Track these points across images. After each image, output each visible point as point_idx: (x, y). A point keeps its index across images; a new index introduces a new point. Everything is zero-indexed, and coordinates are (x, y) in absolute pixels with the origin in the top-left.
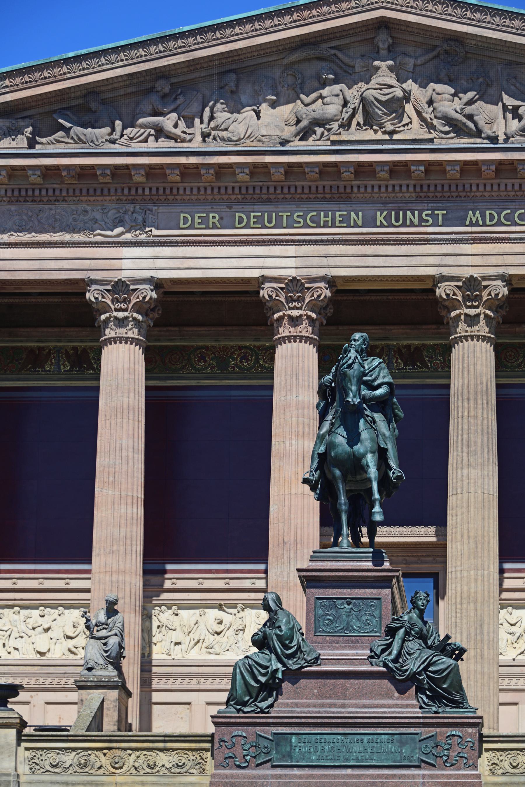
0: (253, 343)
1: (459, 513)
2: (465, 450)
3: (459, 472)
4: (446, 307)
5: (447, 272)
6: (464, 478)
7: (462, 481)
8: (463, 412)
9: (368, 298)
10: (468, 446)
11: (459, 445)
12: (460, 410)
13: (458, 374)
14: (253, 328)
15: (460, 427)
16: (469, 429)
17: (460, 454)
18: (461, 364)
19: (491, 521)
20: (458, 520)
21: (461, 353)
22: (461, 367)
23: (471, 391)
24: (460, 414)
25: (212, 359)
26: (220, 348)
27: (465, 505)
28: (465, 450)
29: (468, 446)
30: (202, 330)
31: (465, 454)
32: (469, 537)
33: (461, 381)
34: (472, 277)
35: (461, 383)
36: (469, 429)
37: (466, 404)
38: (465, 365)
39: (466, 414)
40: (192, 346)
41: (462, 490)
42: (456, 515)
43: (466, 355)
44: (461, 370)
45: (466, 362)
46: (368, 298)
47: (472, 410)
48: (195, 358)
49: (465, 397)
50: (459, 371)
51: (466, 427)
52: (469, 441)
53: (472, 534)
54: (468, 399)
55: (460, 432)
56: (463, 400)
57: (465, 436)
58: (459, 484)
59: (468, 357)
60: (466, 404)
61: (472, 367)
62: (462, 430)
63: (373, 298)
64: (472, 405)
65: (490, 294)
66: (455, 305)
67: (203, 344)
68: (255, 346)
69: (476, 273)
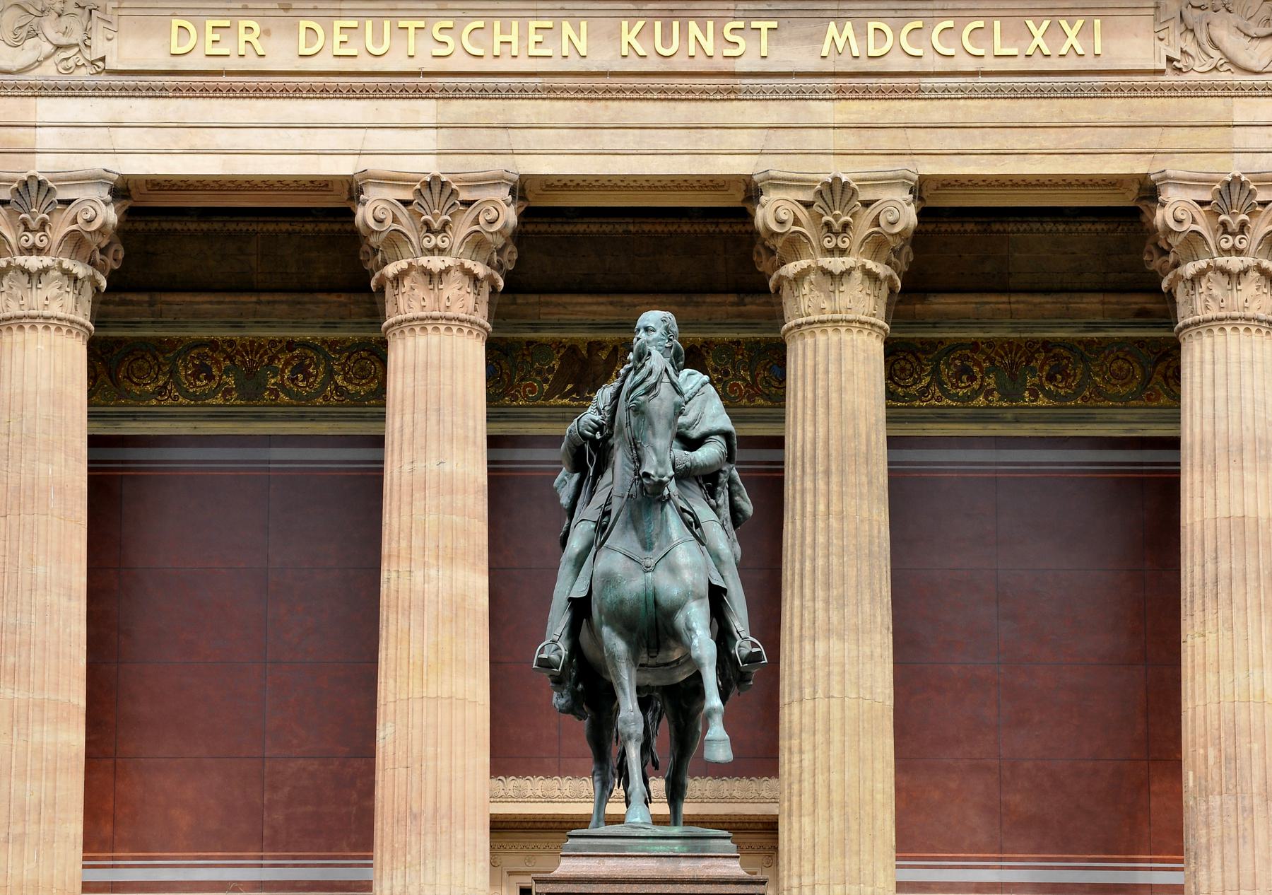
0: (320, 334)
1: (807, 746)
2: (820, 593)
3: (808, 646)
4: (772, 252)
5: (778, 167)
6: (819, 662)
7: (814, 668)
8: (815, 505)
9: (581, 228)
10: (828, 586)
11: (807, 582)
12: (809, 498)
13: (804, 413)
14: (322, 297)
15: (809, 540)
16: (828, 544)
17: (808, 604)
18: (809, 388)
19: (879, 765)
20: (806, 763)
21: (809, 363)
22: (809, 395)
23: (833, 453)
24: (809, 508)
25: (226, 372)
26: (243, 346)
27: (820, 726)
28: (820, 593)
29: (828, 586)
30: (202, 301)
31: (820, 605)
32: (830, 804)
33: (809, 429)
34: (836, 179)
35: (809, 435)
36: (828, 544)
37: (821, 485)
38: (820, 392)
39: (821, 507)
40: (180, 340)
41: (815, 692)
42: (801, 752)
43: (821, 368)
44: (809, 404)
45: (821, 383)
46: (581, 228)
47: (834, 499)
48: (186, 368)
49: (820, 468)
50: (804, 406)
51: (821, 539)
52: (828, 574)
53: (836, 797)
54: (827, 473)
55: (809, 552)
56: (815, 474)
57: (820, 562)
58: (807, 676)
59: (827, 372)
60: (821, 485)
61: (834, 396)
62: (814, 547)
63: (594, 228)
64: (834, 487)
65: (876, 222)
66: (795, 245)
67: (203, 334)
68: (324, 342)
69: (846, 171)
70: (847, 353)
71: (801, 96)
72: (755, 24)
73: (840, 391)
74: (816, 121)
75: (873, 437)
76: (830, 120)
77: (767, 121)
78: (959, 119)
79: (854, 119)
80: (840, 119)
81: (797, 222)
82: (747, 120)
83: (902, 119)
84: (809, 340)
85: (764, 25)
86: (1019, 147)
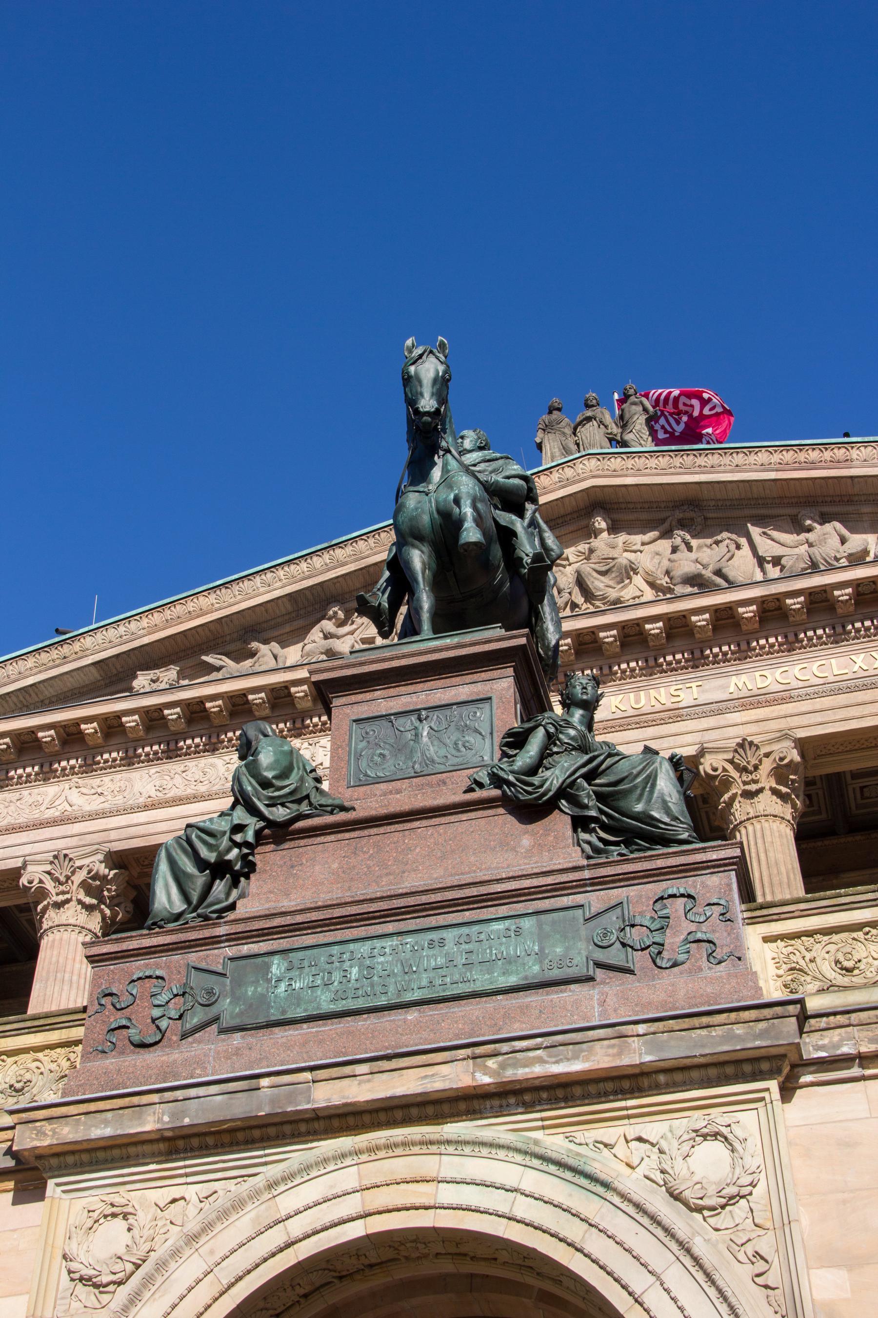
59: (756, 844)
70: (767, 833)
71: (721, 713)
72: (688, 685)
73: (766, 851)
74: (731, 722)
75: (792, 876)
76: (739, 721)
77: (701, 727)
78: (818, 707)
79: (754, 718)
80: (744, 719)
81: (724, 770)
82: (689, 729)
83: (782, 713)
84: (743, 831)
85: (694, 685)
86: (857, 714)
